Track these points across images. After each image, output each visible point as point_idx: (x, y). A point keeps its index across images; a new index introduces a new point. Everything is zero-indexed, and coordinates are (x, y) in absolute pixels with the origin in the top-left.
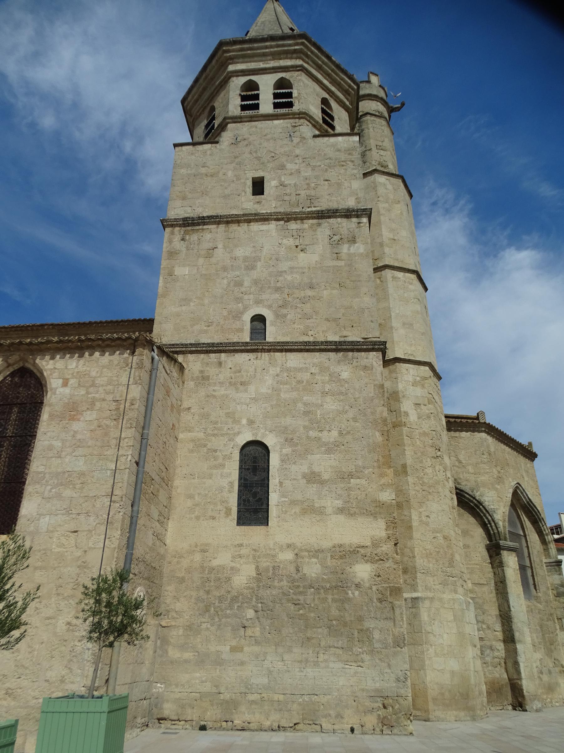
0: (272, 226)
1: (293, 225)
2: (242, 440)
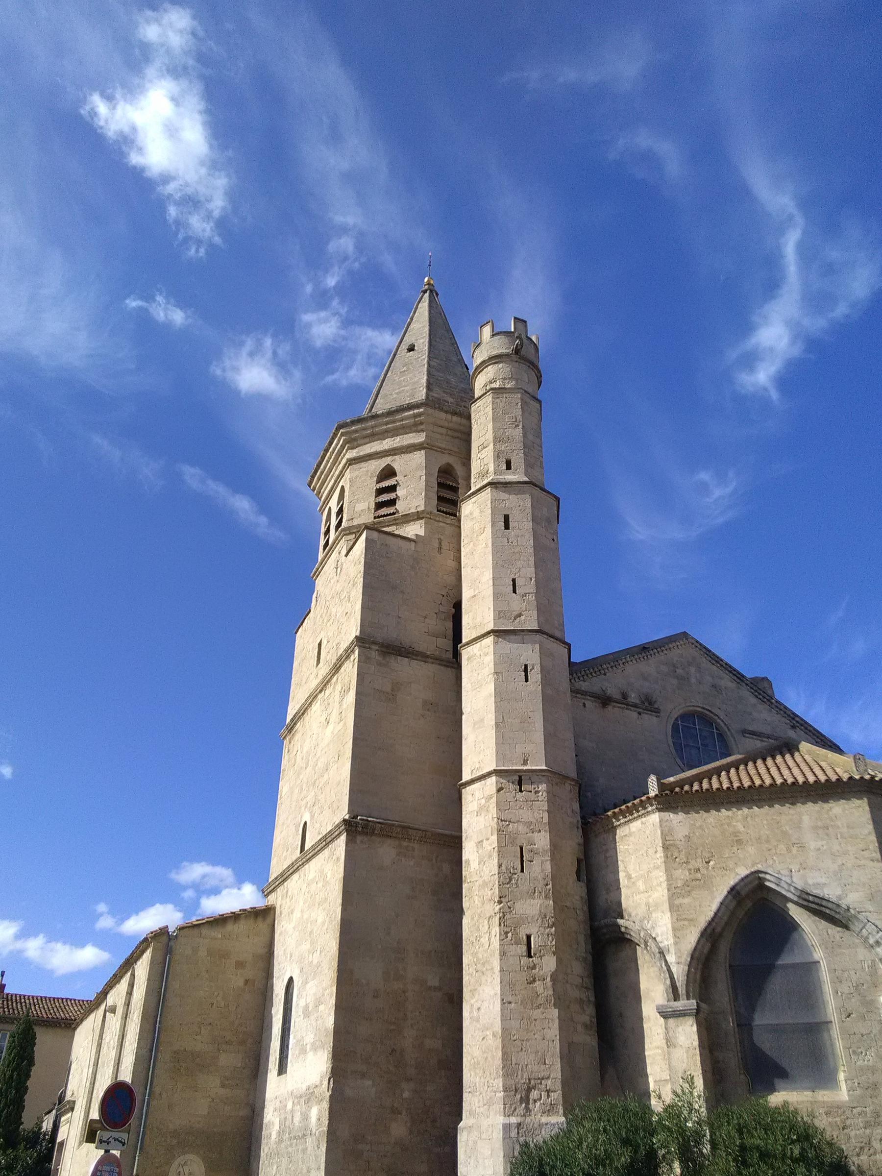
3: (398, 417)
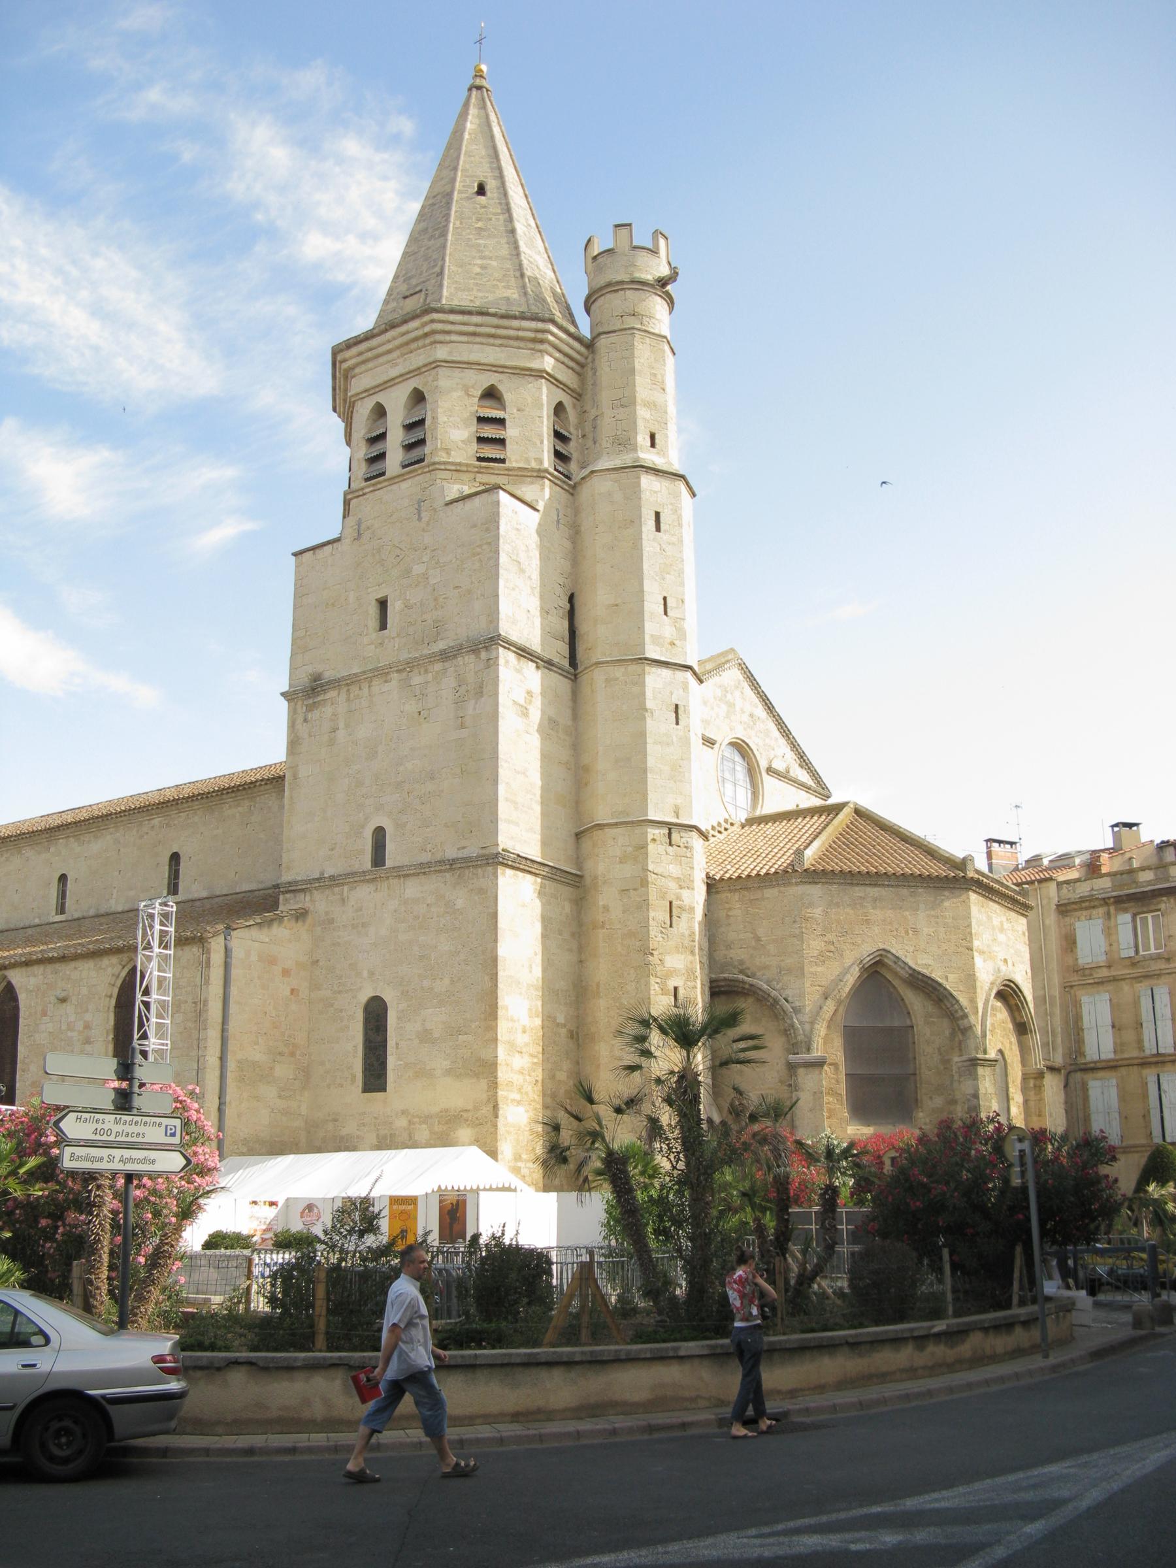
2: (364, 997)
3: (516, 323)
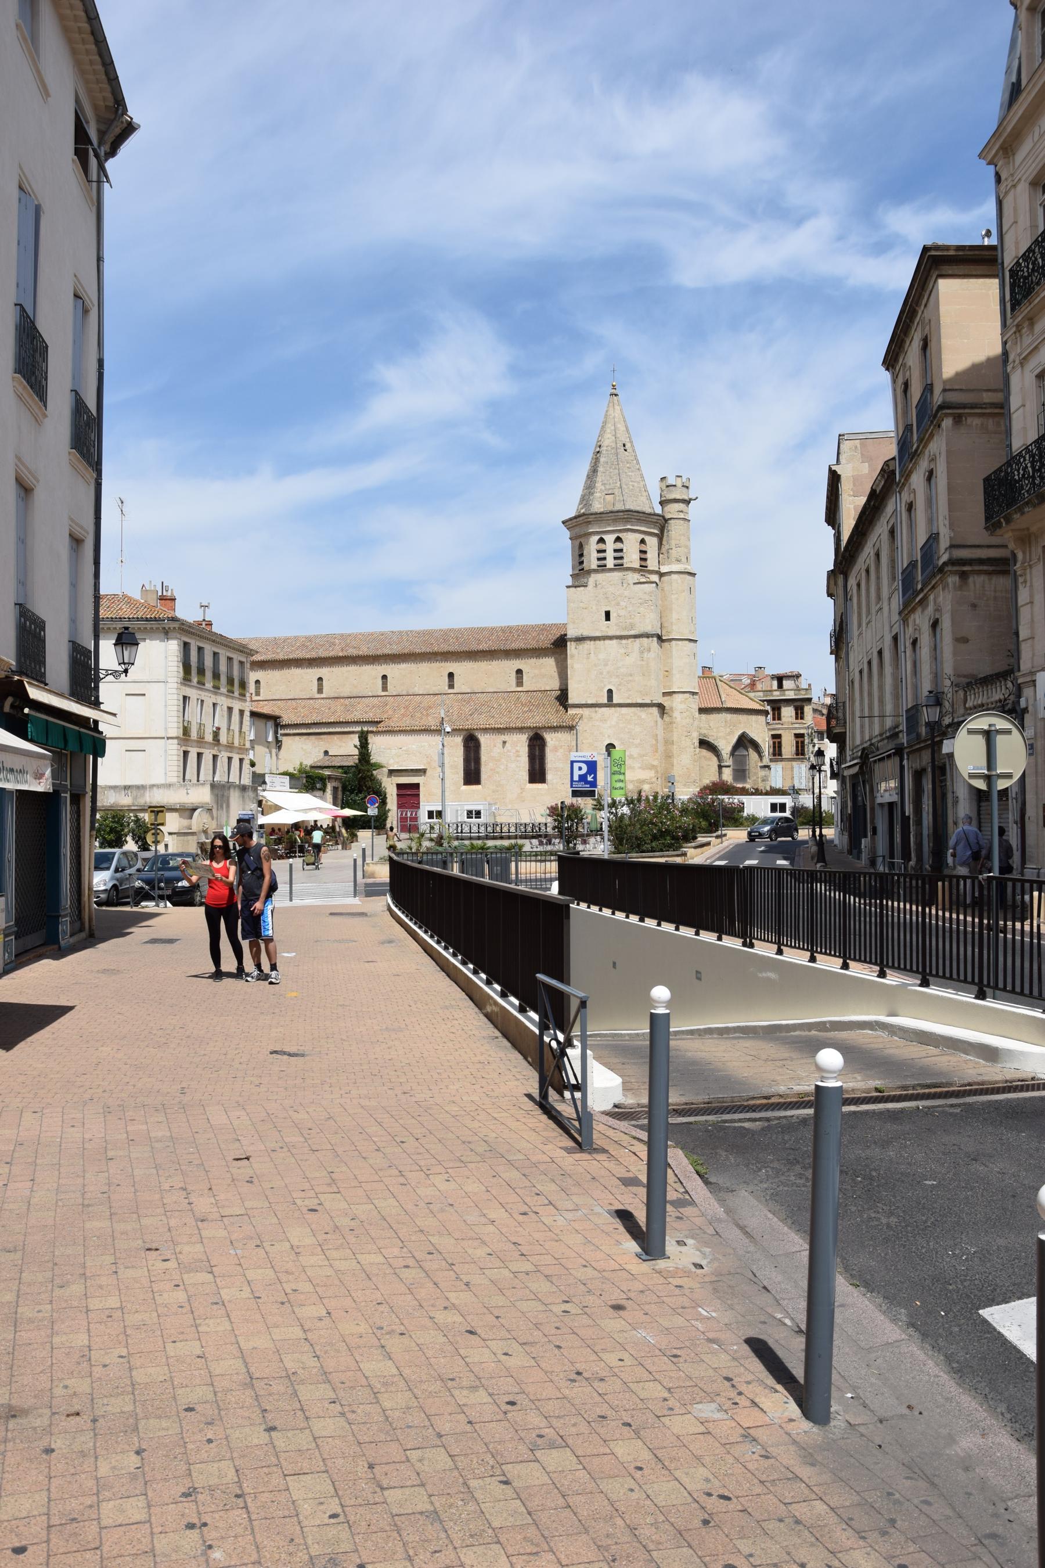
0: (615, 641)
1: (624, 641)
